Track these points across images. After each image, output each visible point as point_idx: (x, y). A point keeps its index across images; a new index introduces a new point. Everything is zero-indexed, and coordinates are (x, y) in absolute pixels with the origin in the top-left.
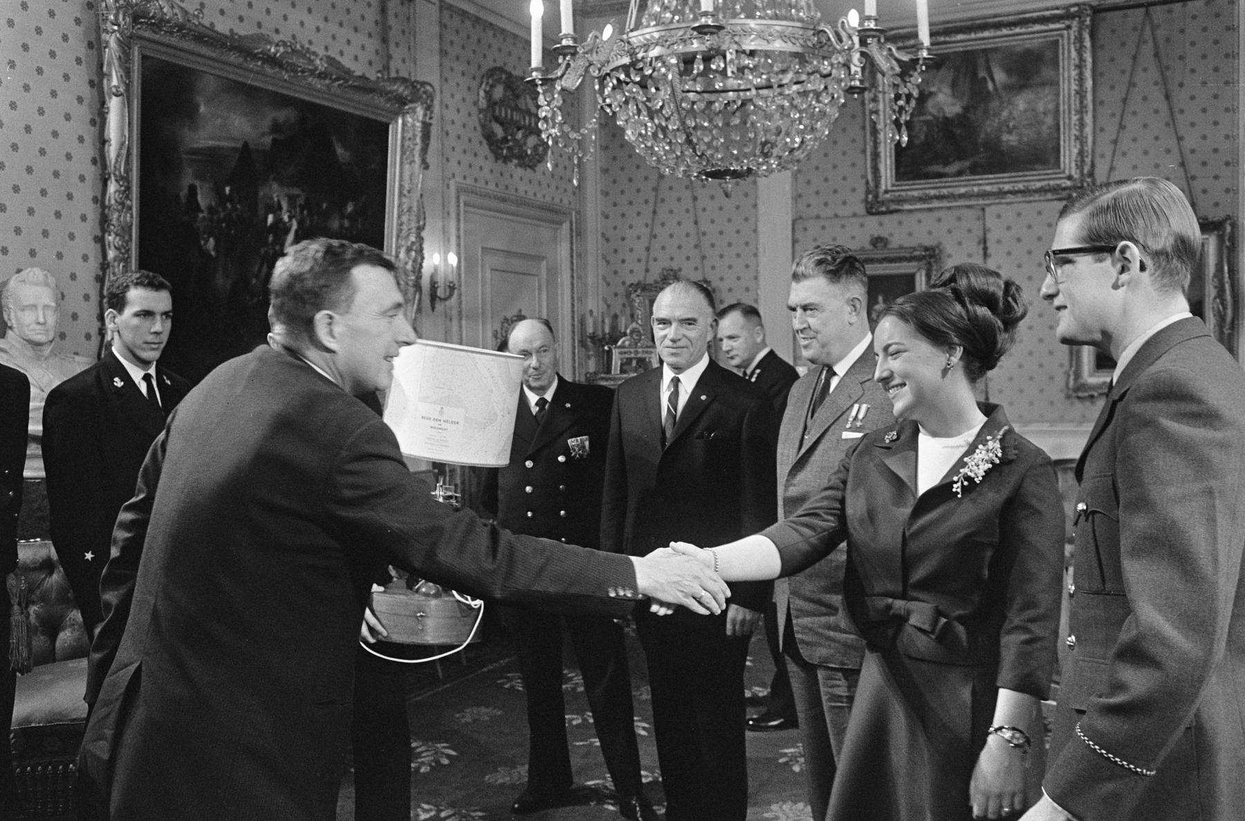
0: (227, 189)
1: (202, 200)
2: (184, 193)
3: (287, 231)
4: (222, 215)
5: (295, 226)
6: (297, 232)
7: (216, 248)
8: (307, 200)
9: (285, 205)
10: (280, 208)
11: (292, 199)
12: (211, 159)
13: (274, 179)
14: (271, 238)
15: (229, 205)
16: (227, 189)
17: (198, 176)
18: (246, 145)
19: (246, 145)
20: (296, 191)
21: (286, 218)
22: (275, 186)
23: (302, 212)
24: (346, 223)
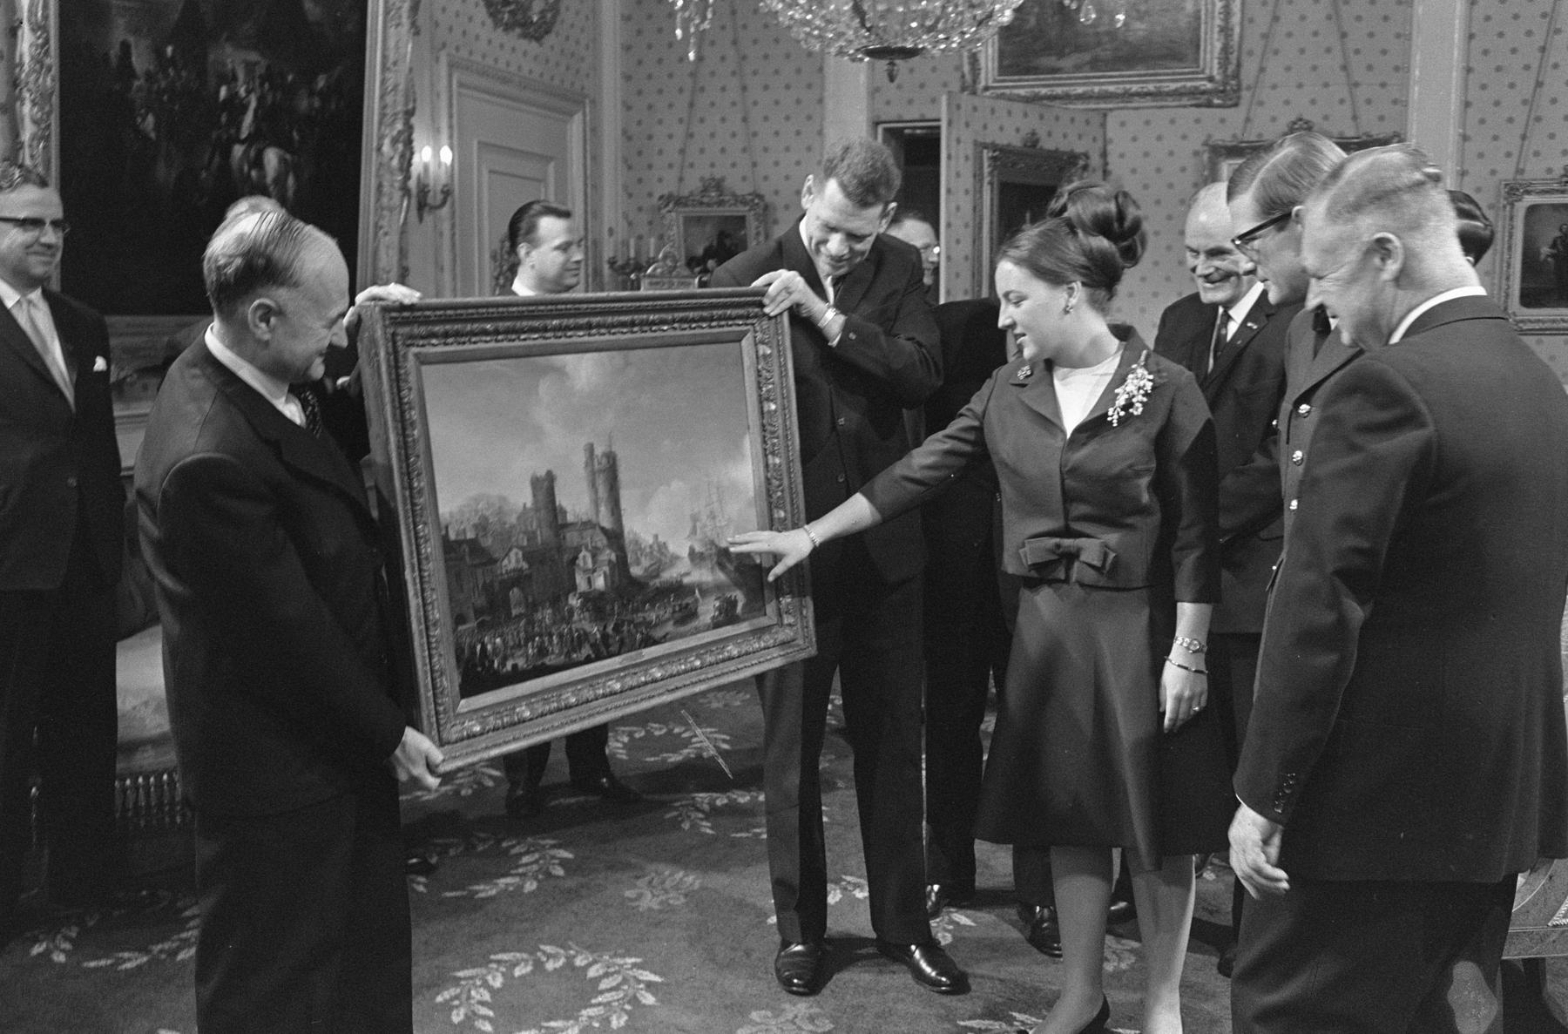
0: (169, 50)
1: (141, 61)
2: (114, 52)
3: (245, 108)
4: (163, 84)
5: (253, 105)
6: (256, 111)
7: (157, 127)
8: (268, 68)
9: (241, 76)
10: (235, 78)
11: (250, 67)
13: (227, 39)
14: (224, 119)
15: (171, 71)
16: (169, 50)
17: (136, 31)
20: (253, 56)
21: (242, 92)
22: (229, 49)
23: (262, 85)
24: (317, 103)
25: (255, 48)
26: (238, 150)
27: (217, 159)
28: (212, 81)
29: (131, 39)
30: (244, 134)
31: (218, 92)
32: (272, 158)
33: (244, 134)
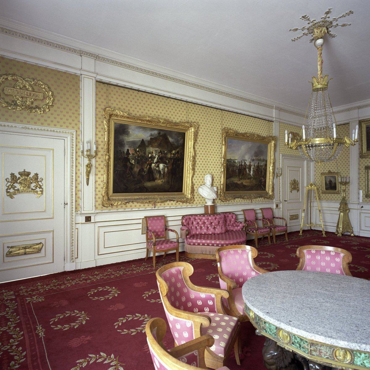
2: (126, 151)
3: (155, 158)
5: (157, 156)
6: (157, 158)
9: (154, 152)
10: (153, 153)
11: (156, 151)
12: (133, 143)
16: (138, 149)
17: (130, 147)
18: (143, 140)
19: (143, 140)
25: (158, 147)
26: (153, 165)
27: (148, 166)
28: (147, 153)
29: (129, 149)
30: (155, 162)
31: (149, 155)
32: (161, 166)
33: (155, 162)
